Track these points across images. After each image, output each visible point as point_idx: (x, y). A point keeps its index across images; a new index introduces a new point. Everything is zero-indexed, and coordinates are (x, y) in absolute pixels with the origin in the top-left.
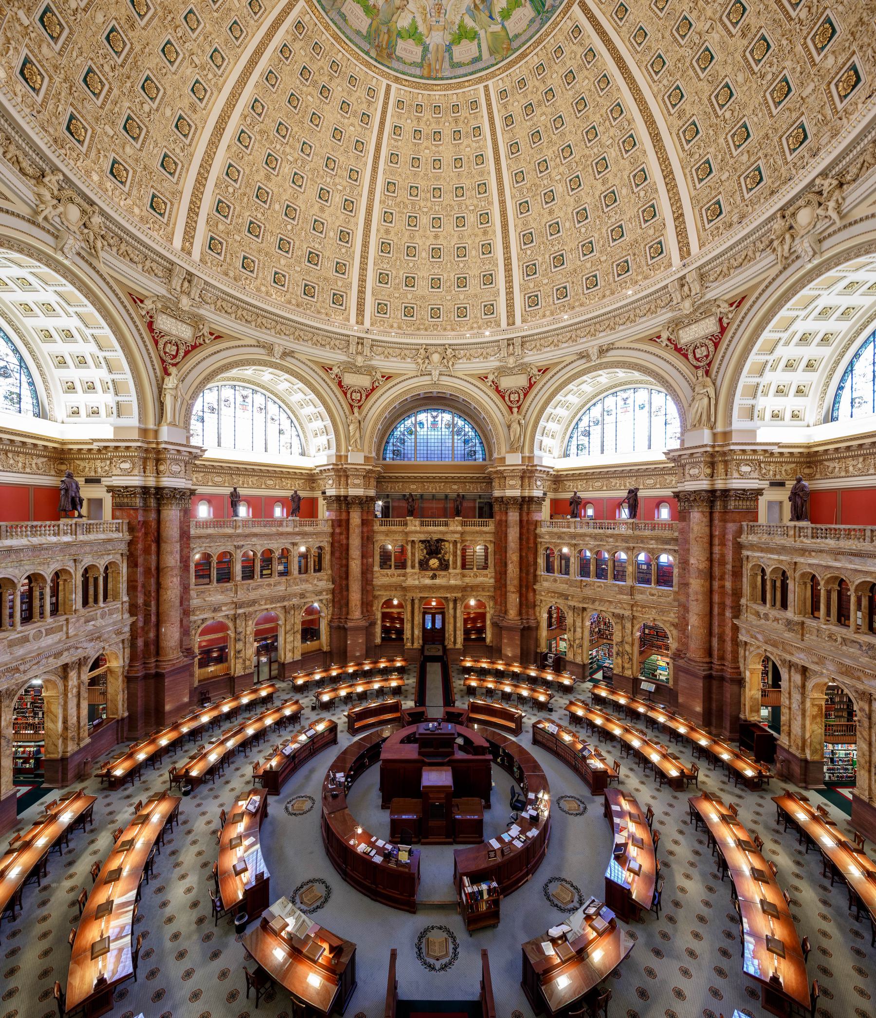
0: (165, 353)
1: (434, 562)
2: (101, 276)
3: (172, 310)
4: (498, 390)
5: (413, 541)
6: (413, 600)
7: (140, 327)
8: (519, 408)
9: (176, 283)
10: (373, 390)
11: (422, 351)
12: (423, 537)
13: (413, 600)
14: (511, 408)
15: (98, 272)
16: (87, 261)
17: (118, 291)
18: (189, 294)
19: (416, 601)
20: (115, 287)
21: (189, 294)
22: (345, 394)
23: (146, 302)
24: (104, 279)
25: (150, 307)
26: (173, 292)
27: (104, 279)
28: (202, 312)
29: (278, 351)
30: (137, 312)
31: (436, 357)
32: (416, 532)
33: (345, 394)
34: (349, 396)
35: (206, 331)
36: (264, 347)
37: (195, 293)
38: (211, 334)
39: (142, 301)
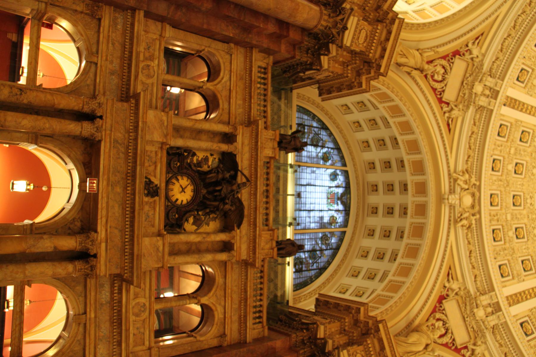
1: (182, 192)
5: (229, 138)
6: (90, 117)
10: (440, 101)
12: (243, 162)
13: (90, 117)
19: (86, 129)
22: (444, 58)
32: (255, 149)
34: (444, 62)
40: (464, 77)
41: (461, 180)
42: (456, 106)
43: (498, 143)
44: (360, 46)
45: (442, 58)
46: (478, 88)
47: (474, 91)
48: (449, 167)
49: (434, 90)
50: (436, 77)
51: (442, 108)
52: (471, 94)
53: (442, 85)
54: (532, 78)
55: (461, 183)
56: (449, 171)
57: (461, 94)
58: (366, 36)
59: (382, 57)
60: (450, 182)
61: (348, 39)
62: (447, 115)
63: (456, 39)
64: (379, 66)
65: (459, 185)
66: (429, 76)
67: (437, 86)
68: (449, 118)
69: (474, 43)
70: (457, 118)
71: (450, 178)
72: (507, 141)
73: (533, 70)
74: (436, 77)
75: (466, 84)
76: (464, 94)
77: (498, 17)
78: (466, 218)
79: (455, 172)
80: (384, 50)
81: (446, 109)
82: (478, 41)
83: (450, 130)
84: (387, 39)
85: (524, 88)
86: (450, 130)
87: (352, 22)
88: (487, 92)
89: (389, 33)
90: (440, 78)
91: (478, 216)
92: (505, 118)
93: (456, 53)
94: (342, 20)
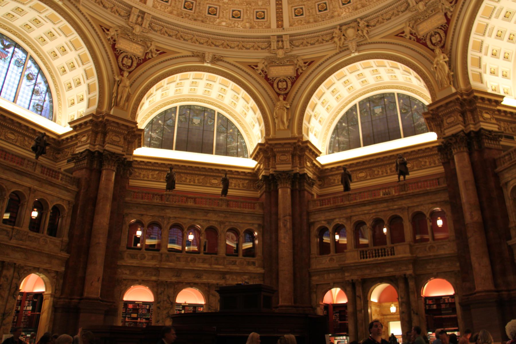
0: (123, 64)
2: (82, 14)
3: (127, 33)
4: (418, 40)
7: (106, 45)
8: (443, 47)
9: (133, 18)
10: (298, 76)
11: (337, 31)
14: (433, 50)
15: (80, 11)
16: (74, 5)
17: (92, 23)
18: (141, 25)
20: (91, 20)
21: (141, 25)
22: (272, 85)
23: (111, 30)
24: (84, 16)
25: (112, 34)
26: (130, 23)
27: (84, 16)
28: (149, 35)
29: (209, 57)
30: (105, 38)
31: (350, 32)
33: (272, 85)
34: (275, 86)
35: (153, 48)
36: (198, 56)
37: (146, 24)
38: (157, 51)
39: (108, 30)
40: (278, 65)
41: (340, 44)
42: (296, 65)
43: (308, 14)
44: (289, 157)
45: (273, 87)
46: (281, 53)
47: (283, 56)
48: (334, 55)
49: (293, 84)
50: (285, 86)
51: (301, 73)
52: (285, 58)
53: (288, 80)
54: (259, 7)
55: (342, 43)
56: (337, 54)
57: (288, 64)
58: (282, 155)
59: (289, 143)
60: (343, 51)
61: (287, 167)
62: (304, 69)
63: (260, 84)
64: (295, 143)
65: (343, 44)
66: (286, 92)
67: (290, 85)
68: (305, 67)
69: (258, 70)
70: (302, 59)
71: (341, 52)
72: (304, 5)
73: (254, 9)
74: (285, 86)
75: (281, 63)
76: (287, 61)
77: (236, 62)
78: (362, 32)
79: (336, 49)
80: (285, 144)
81: (300, 71)
82: (255, 67)
83: (312, 62)
84: (280, 144)
85: (267, 10)
86: (312, 62)
87: (280, 168)
88: (280, 43)
89: (276, 144)
90: (285, 83)
91: (359, 20)
92: (291, 15)
93: (267, 78)
94: (280, 174)
